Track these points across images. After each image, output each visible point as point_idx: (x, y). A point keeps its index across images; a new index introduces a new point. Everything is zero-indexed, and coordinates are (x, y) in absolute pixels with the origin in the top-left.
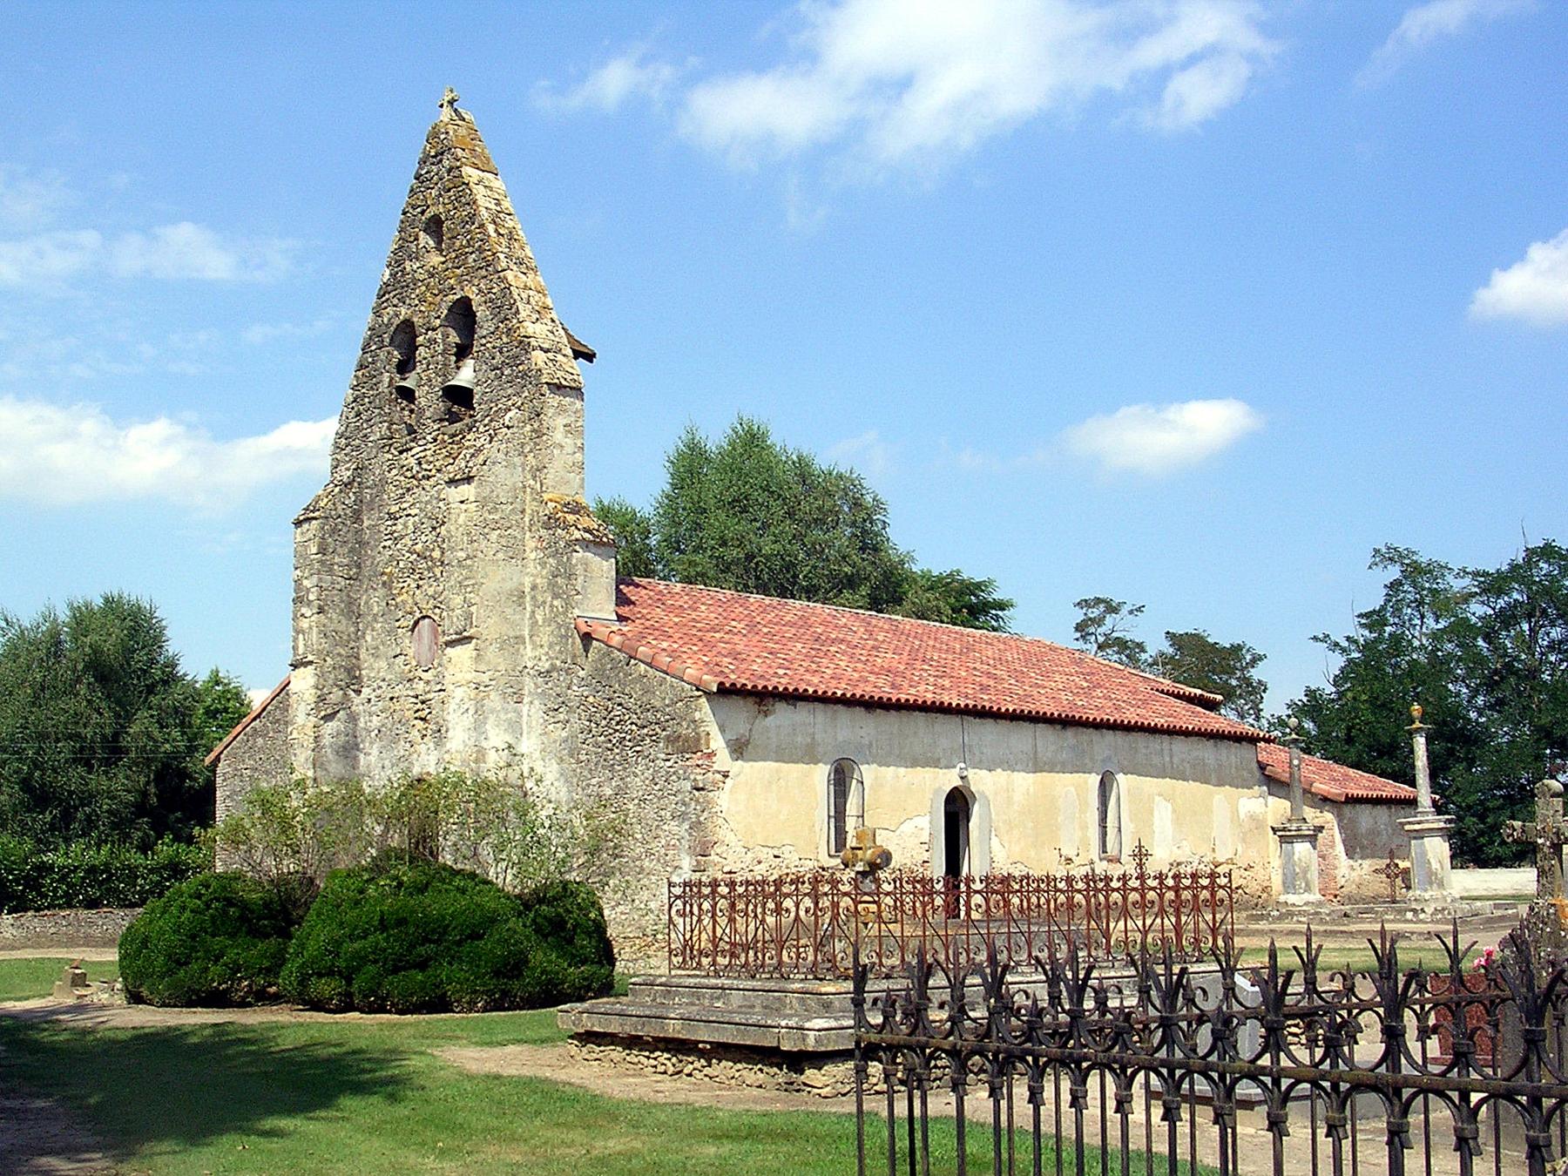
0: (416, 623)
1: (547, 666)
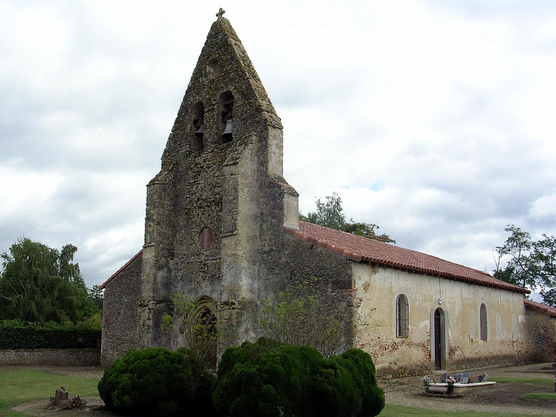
0: (202, 230)
1: (268, 249)
